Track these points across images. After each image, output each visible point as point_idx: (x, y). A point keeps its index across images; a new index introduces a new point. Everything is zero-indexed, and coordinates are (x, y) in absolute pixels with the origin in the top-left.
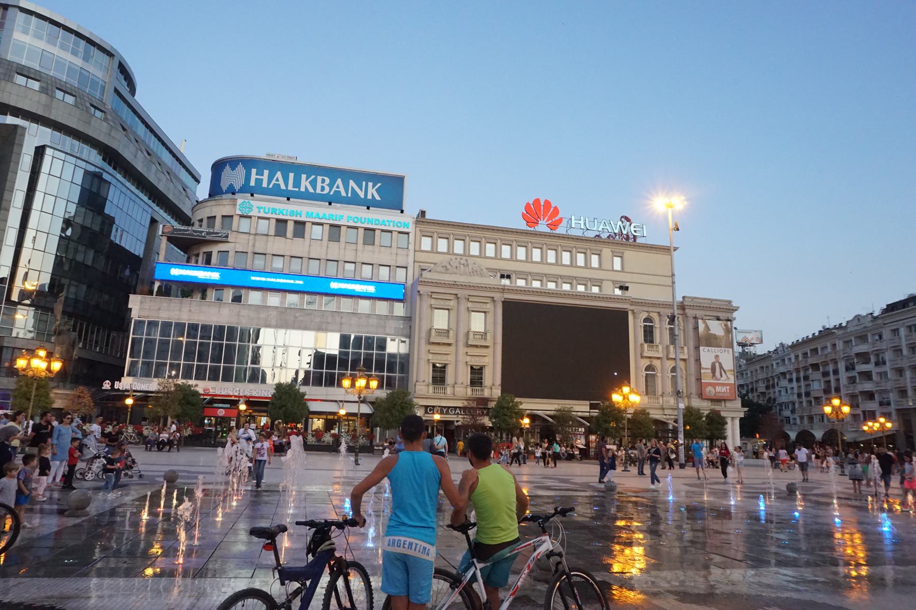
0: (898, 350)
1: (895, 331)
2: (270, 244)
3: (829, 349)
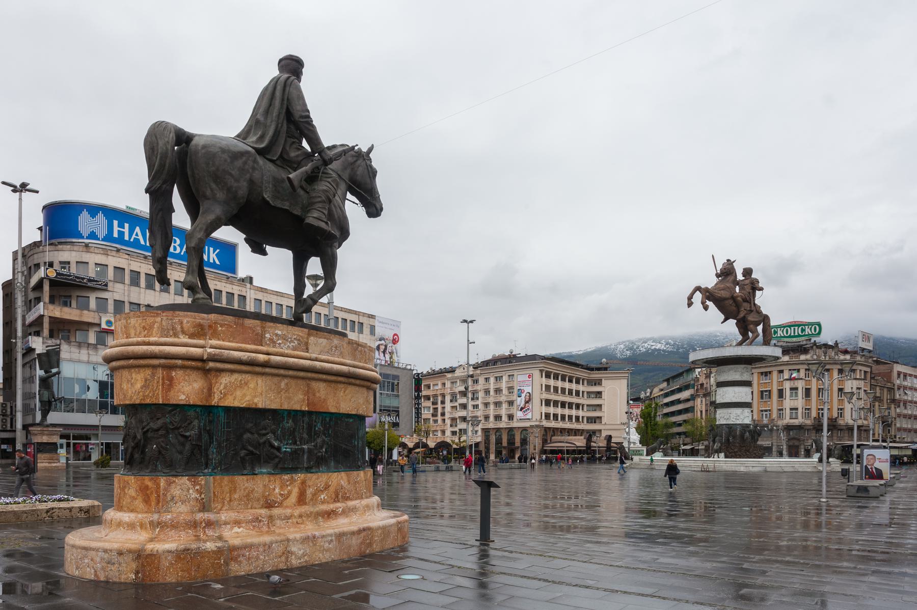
0: (487, 392)
1: (487, 379)
2: (142, 295)
3: (440, 386)
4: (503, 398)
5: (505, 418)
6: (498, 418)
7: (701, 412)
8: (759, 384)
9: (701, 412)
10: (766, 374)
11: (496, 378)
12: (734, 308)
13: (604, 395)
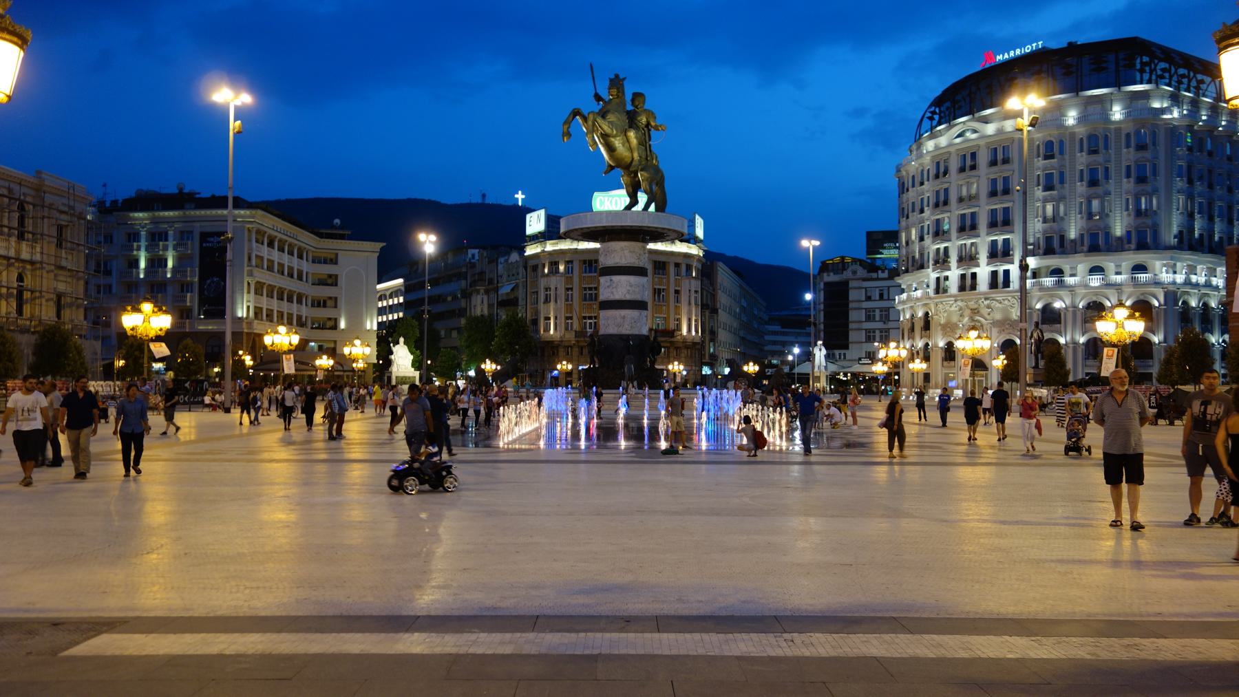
13: (342, 281)
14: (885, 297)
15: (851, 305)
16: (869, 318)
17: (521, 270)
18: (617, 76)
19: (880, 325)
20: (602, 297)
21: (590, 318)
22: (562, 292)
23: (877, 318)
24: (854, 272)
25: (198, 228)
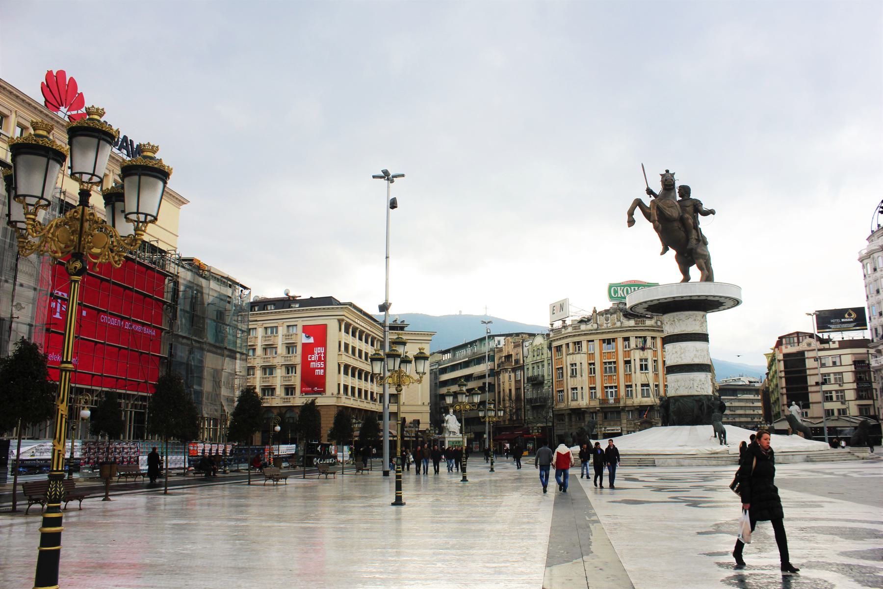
4: (278, 361)
5: (280, 391)
6: (269, 390)
7: (510, 390)
8: (601, 353)
9: (510, 390)
10: (609, 341)
11: (266, 328)
12: (682, 234)
14: (838, 364)
15: (808, 372)
16: (825, 382)
17: (546, 350)
18: (667, 171)
19: (836, 387)
20: (668, 363)
21: (611, 387)
22: (585, 366)
23: (833, 381)
24: (809, 345)
25: (301, 323)
